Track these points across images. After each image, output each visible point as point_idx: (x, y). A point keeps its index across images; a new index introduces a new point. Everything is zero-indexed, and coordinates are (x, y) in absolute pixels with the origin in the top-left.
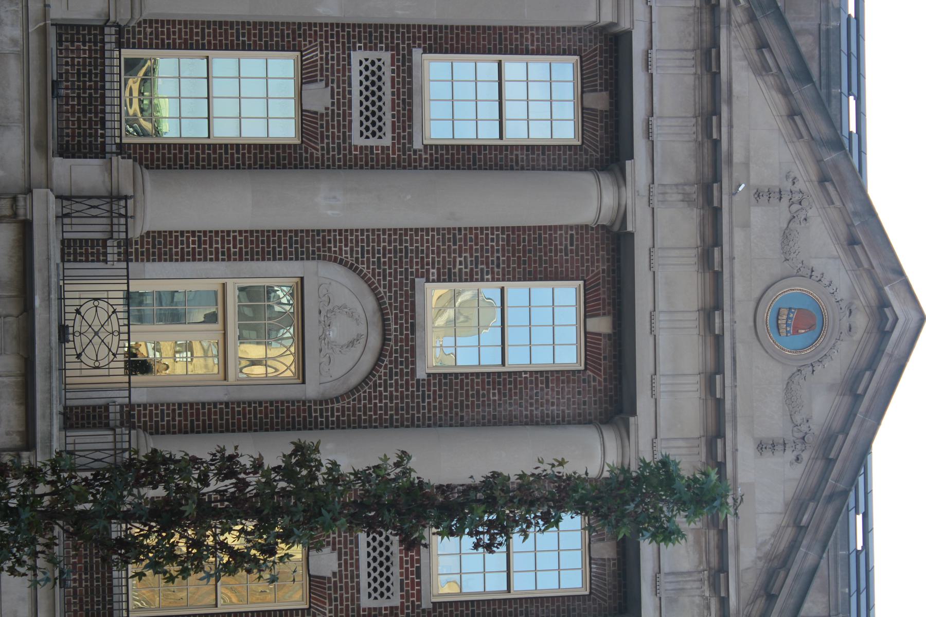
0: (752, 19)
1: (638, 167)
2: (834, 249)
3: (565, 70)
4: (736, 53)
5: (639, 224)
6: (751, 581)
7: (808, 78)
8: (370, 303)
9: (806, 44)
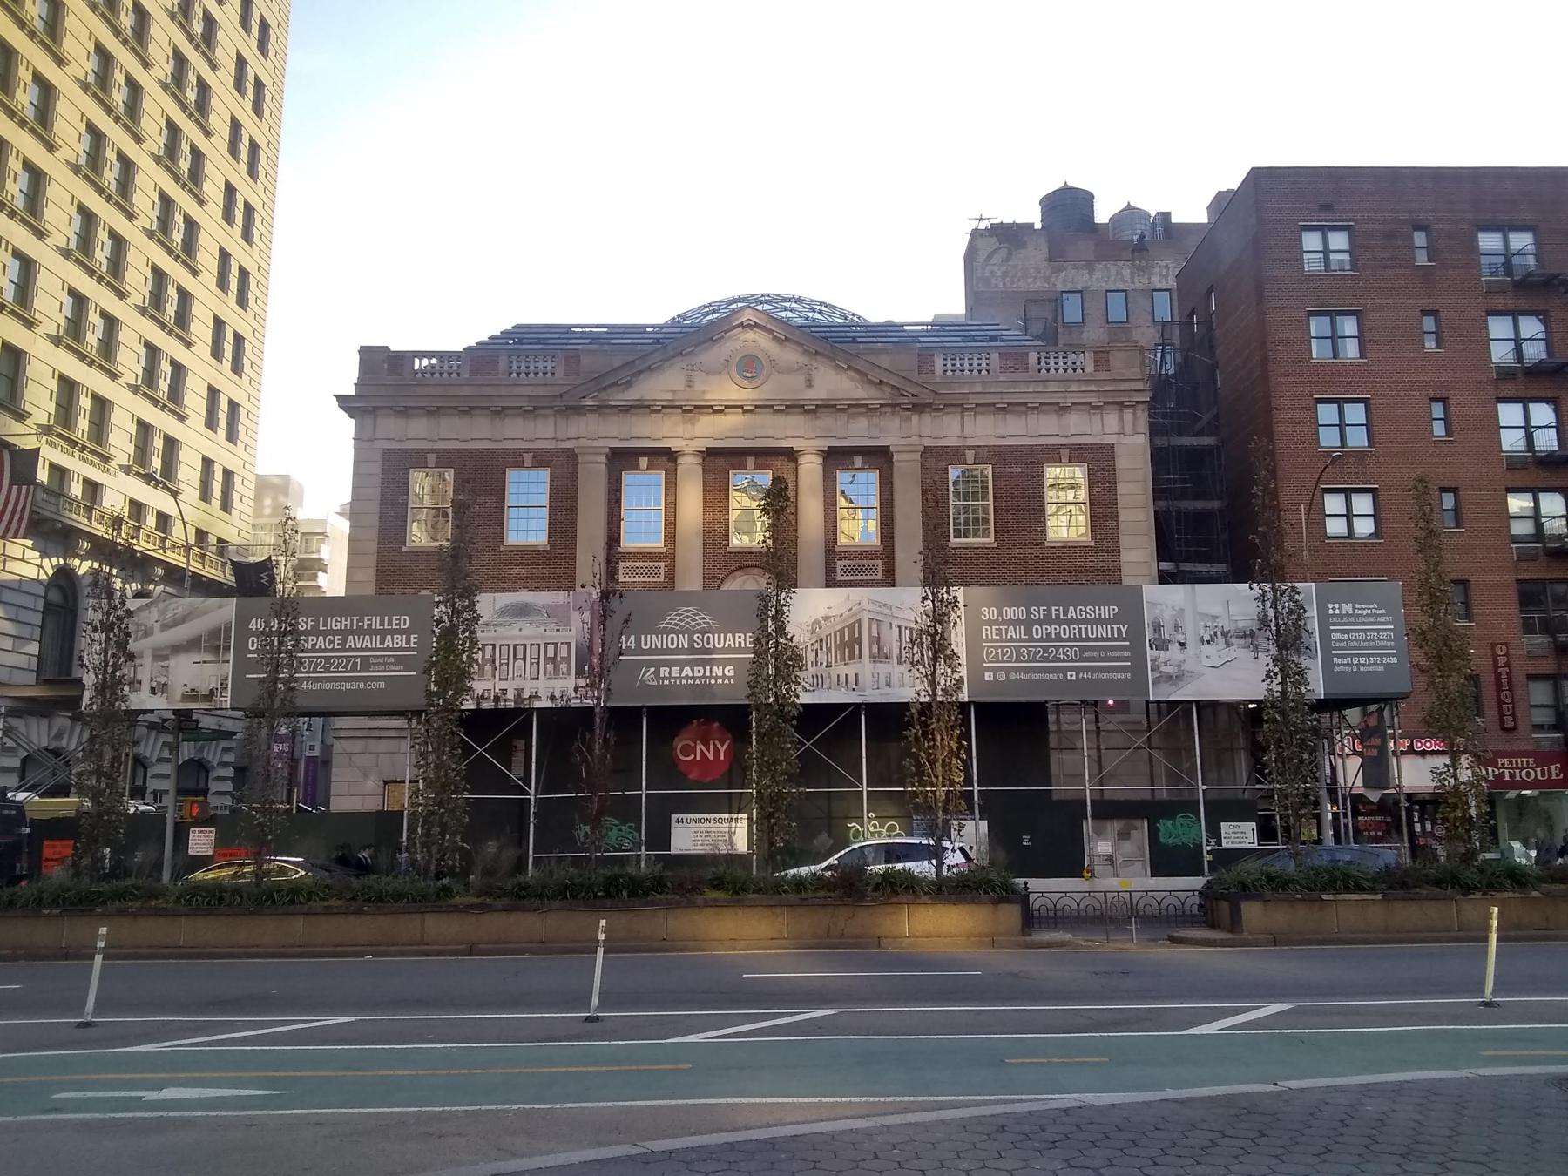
0: (604, 389)
1: (675, 445)
2: (716, 349)
3: (628, 478)
4: (620, 397)
5: (702, 445)
6: (873, 392)
7: (633, 362)
8: (738, 573)
9: (617, 362)
